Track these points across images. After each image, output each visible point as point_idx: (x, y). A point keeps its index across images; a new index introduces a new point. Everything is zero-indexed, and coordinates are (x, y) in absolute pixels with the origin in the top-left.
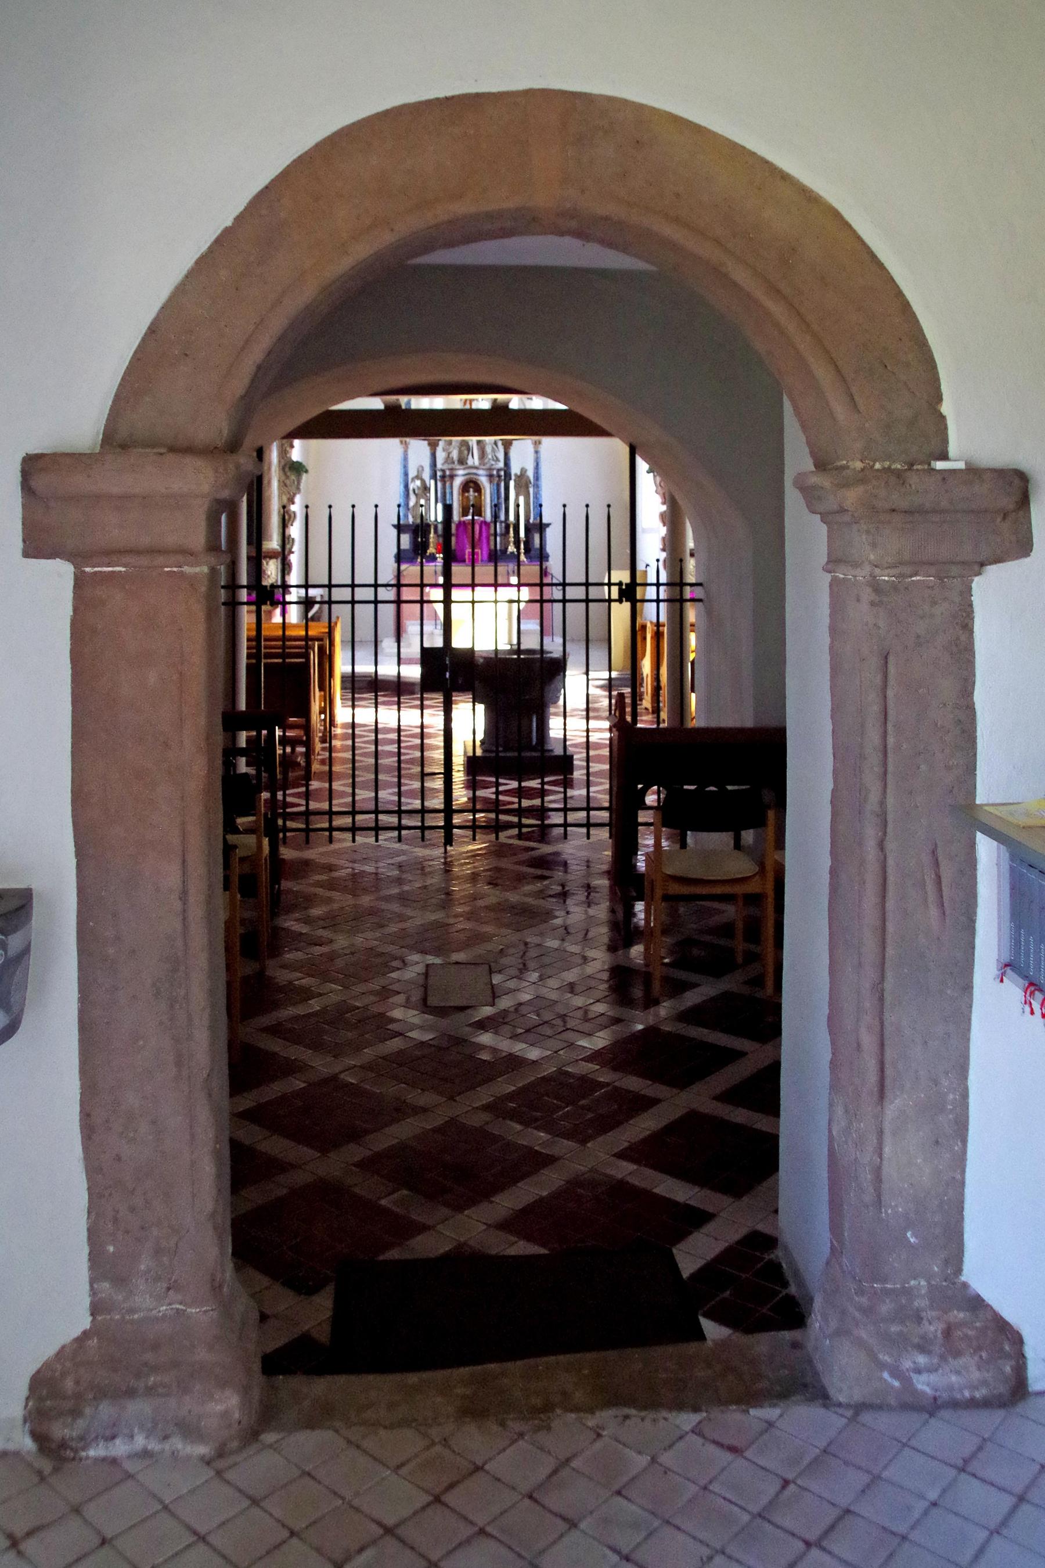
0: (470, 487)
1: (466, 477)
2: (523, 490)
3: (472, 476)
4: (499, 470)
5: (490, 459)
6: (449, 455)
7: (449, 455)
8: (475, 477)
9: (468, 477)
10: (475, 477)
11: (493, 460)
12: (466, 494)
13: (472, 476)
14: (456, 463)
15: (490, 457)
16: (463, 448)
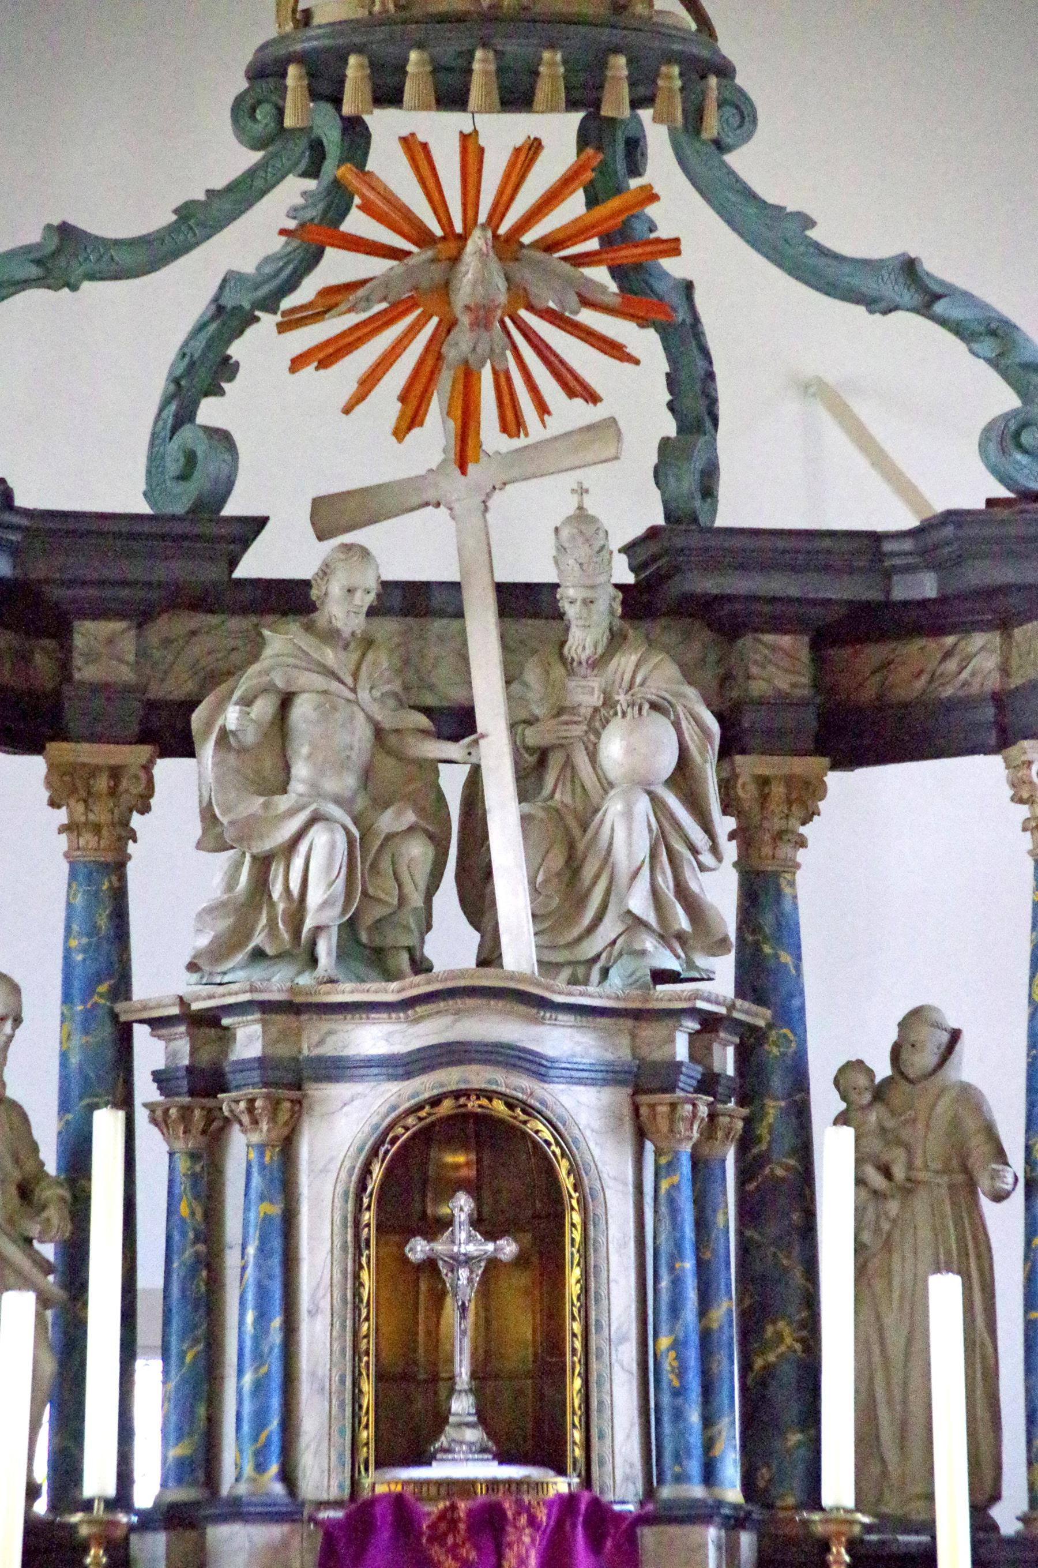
0: (451, 1187)
1: (425, 1085)
2: (921, 1204)
3: (477, 1076)
4: (710, 1023)
5: (637, 922)
6: (261, 884)
7: (261, 884)
8: (520, 1084)
9: (451, 1077)
10: (520, 1084)
11: (668, 937)
12: (418, 1249)
13: (477, 1076)
14: (325, 949)
15: (639, 902)
16: (388, 821)
